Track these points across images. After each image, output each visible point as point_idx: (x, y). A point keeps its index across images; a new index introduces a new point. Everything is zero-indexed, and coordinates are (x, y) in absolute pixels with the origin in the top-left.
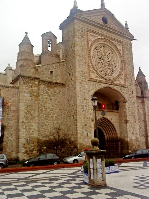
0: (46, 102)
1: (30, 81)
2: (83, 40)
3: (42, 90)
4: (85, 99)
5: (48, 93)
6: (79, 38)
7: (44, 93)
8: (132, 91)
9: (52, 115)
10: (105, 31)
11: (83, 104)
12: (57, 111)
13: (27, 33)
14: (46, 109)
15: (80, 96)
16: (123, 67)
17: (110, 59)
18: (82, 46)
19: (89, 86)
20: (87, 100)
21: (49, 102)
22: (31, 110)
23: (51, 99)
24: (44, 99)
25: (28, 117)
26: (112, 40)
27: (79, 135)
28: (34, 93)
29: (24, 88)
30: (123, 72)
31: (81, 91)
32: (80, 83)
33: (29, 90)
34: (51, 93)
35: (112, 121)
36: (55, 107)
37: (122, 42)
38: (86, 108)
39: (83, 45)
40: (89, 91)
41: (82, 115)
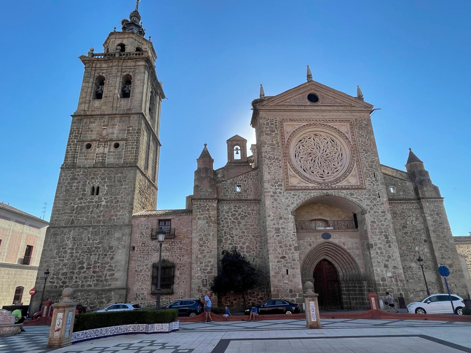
0: (232, 228)
1: (205, 204)
2: (274, 135)
3: (226, 213)
4: (281, 218)
5: (236, 215)
6: (267, 134)
7: (228, 216)
8: (377, 193)
9: (241, 245)
10: (315, 113)
11: (276, 226)
12: (249, 238)
13: (205, 145)
14: (232, 237)
15: (272, 215)
16: (355, 158)
17: (328, 151)
19: (288, 198)
20: (285, 219)
21: (237, 227)
22: (207, 240)
23: (239, 223)
24: (229, 224)
25: (203, 250)
26: (328, 122)
27: (272, 273)
28: (212, 218)
29: (198, 213)
30: (355, 164)
31: (273, 207)
32: (272, 196)
33: (205, 215)
34: (239, 214)
35: (345, 247)
37: (349, 121)
38: (284, 232)
39: (274, 142)
40: (289, 206)
41: (277, 243)
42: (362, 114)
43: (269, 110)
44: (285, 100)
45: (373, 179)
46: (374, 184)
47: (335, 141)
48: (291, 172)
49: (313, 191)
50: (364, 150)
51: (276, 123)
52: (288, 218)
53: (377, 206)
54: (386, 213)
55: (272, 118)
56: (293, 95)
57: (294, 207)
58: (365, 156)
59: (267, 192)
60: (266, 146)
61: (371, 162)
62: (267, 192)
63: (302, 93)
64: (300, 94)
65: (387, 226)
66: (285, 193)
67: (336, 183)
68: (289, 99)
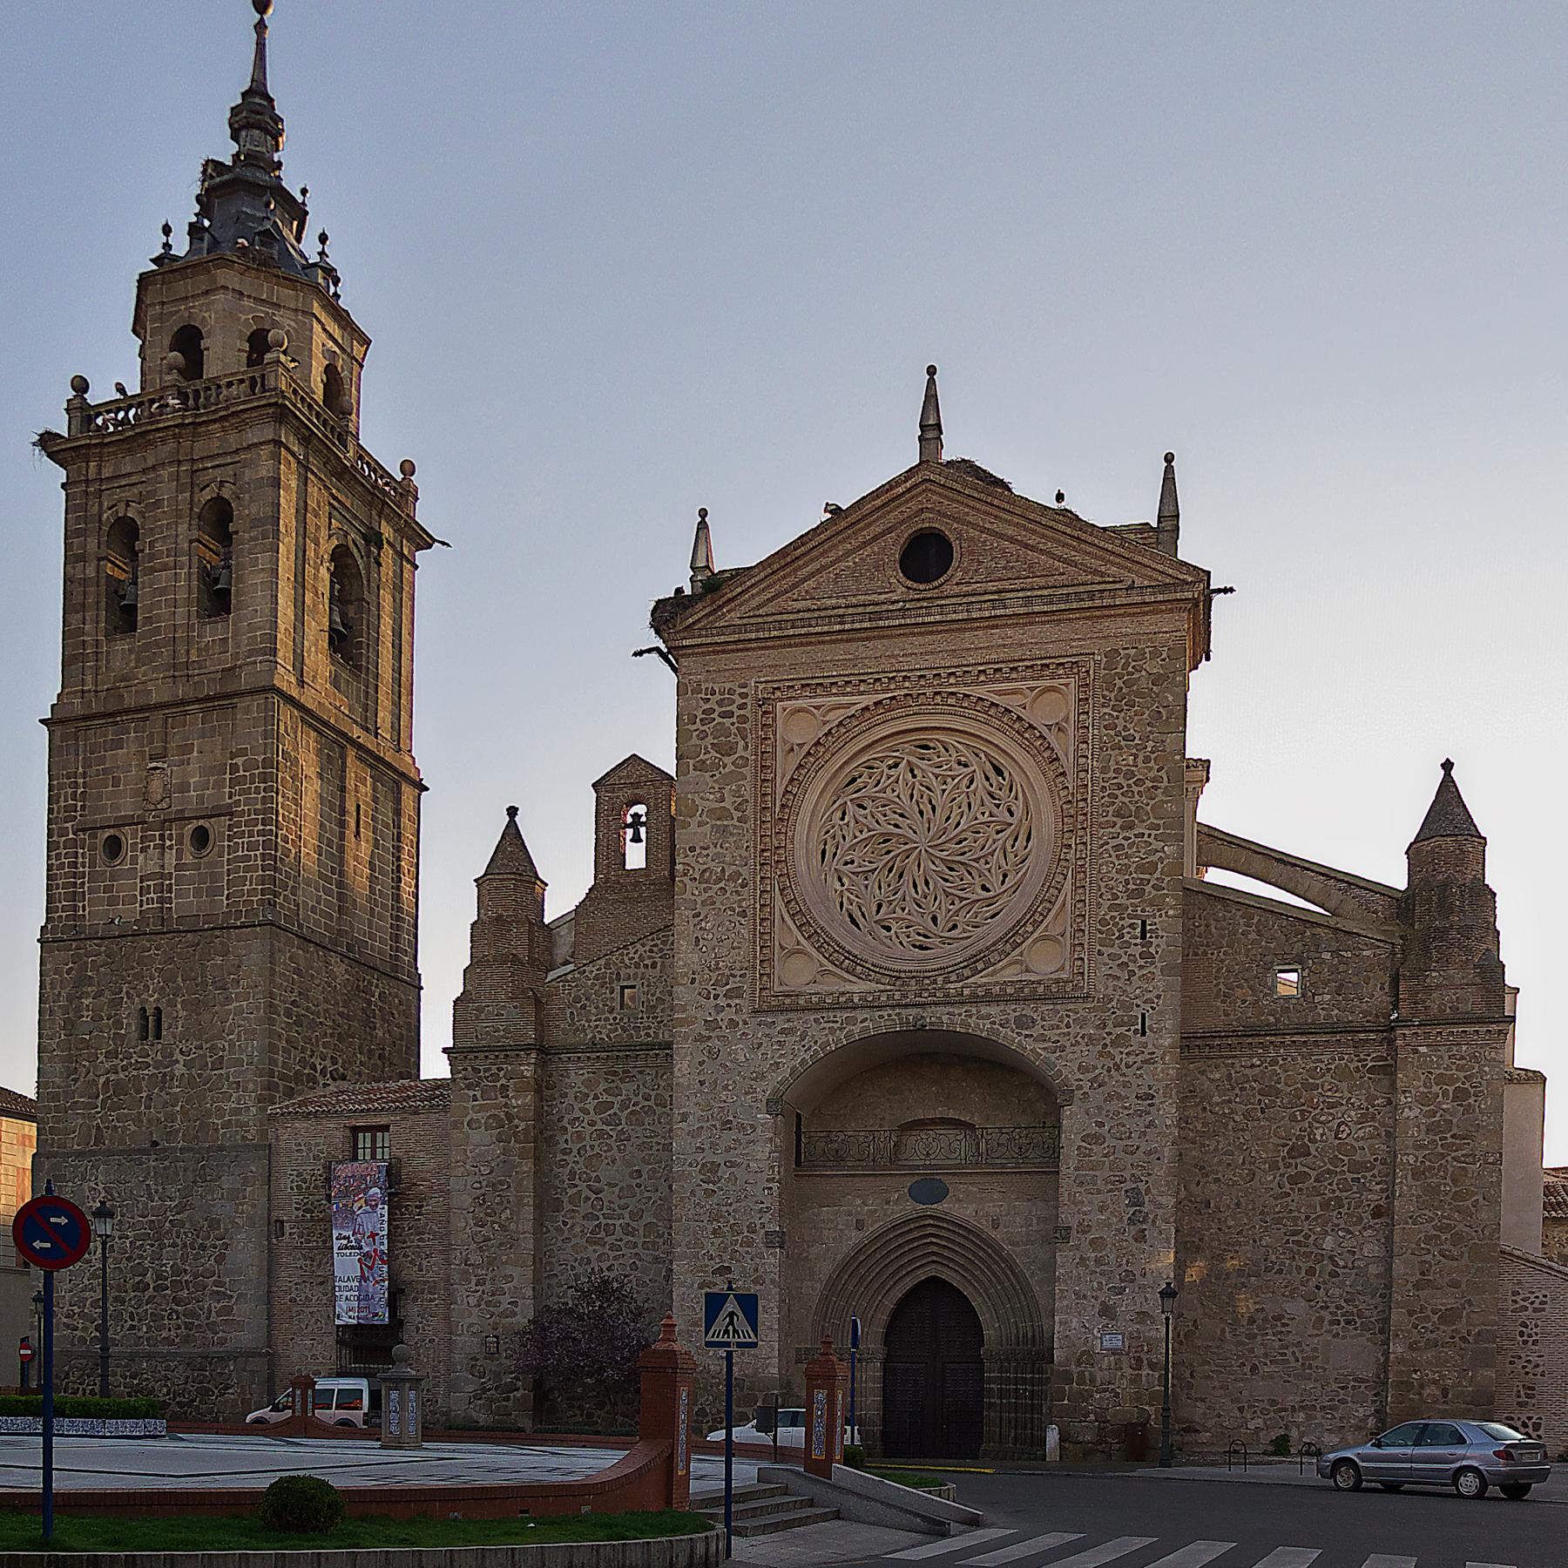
2: (730, 768)
3: (576, 1097)
18: (723, 814)
21: (615, 1152)
23: (623, 1138)
31: (702, 1083)
32: (700, 1039)
36: (645, 1176)
40: (761, 1076)
42: (1149, 623)
43: (721, 648)
44: (795, 586)
45: (1133, 950)
46: (1132, 973)
47: (1006, 774)
48: (788, 934)
49: (860, 1015)
50: (1118, 814)
51: (742, 707)
52: (752, 1126)
53: (1125, 1070)
54: (1156, 1101)
55: (728, 686)
56: (833, 555)
57: (781, 1083)
58: (1120, 841)
59: (682, 1022)
60: (694, 821)
61: (1141, 868)
62: (682, 1022)
63: (875, 539)
64: (865, 544)
65: (1149, 1153)
66: (753, 1022)
67: (967, 972)
68: (812, 575)
